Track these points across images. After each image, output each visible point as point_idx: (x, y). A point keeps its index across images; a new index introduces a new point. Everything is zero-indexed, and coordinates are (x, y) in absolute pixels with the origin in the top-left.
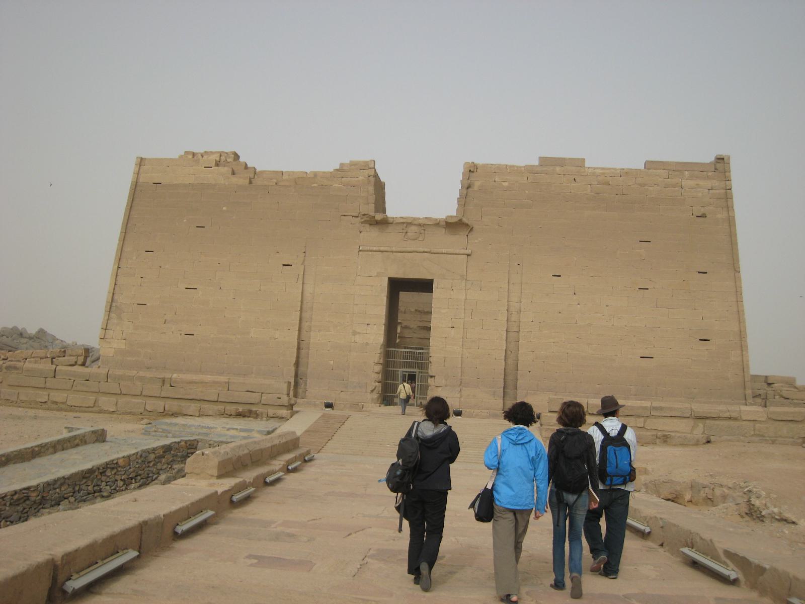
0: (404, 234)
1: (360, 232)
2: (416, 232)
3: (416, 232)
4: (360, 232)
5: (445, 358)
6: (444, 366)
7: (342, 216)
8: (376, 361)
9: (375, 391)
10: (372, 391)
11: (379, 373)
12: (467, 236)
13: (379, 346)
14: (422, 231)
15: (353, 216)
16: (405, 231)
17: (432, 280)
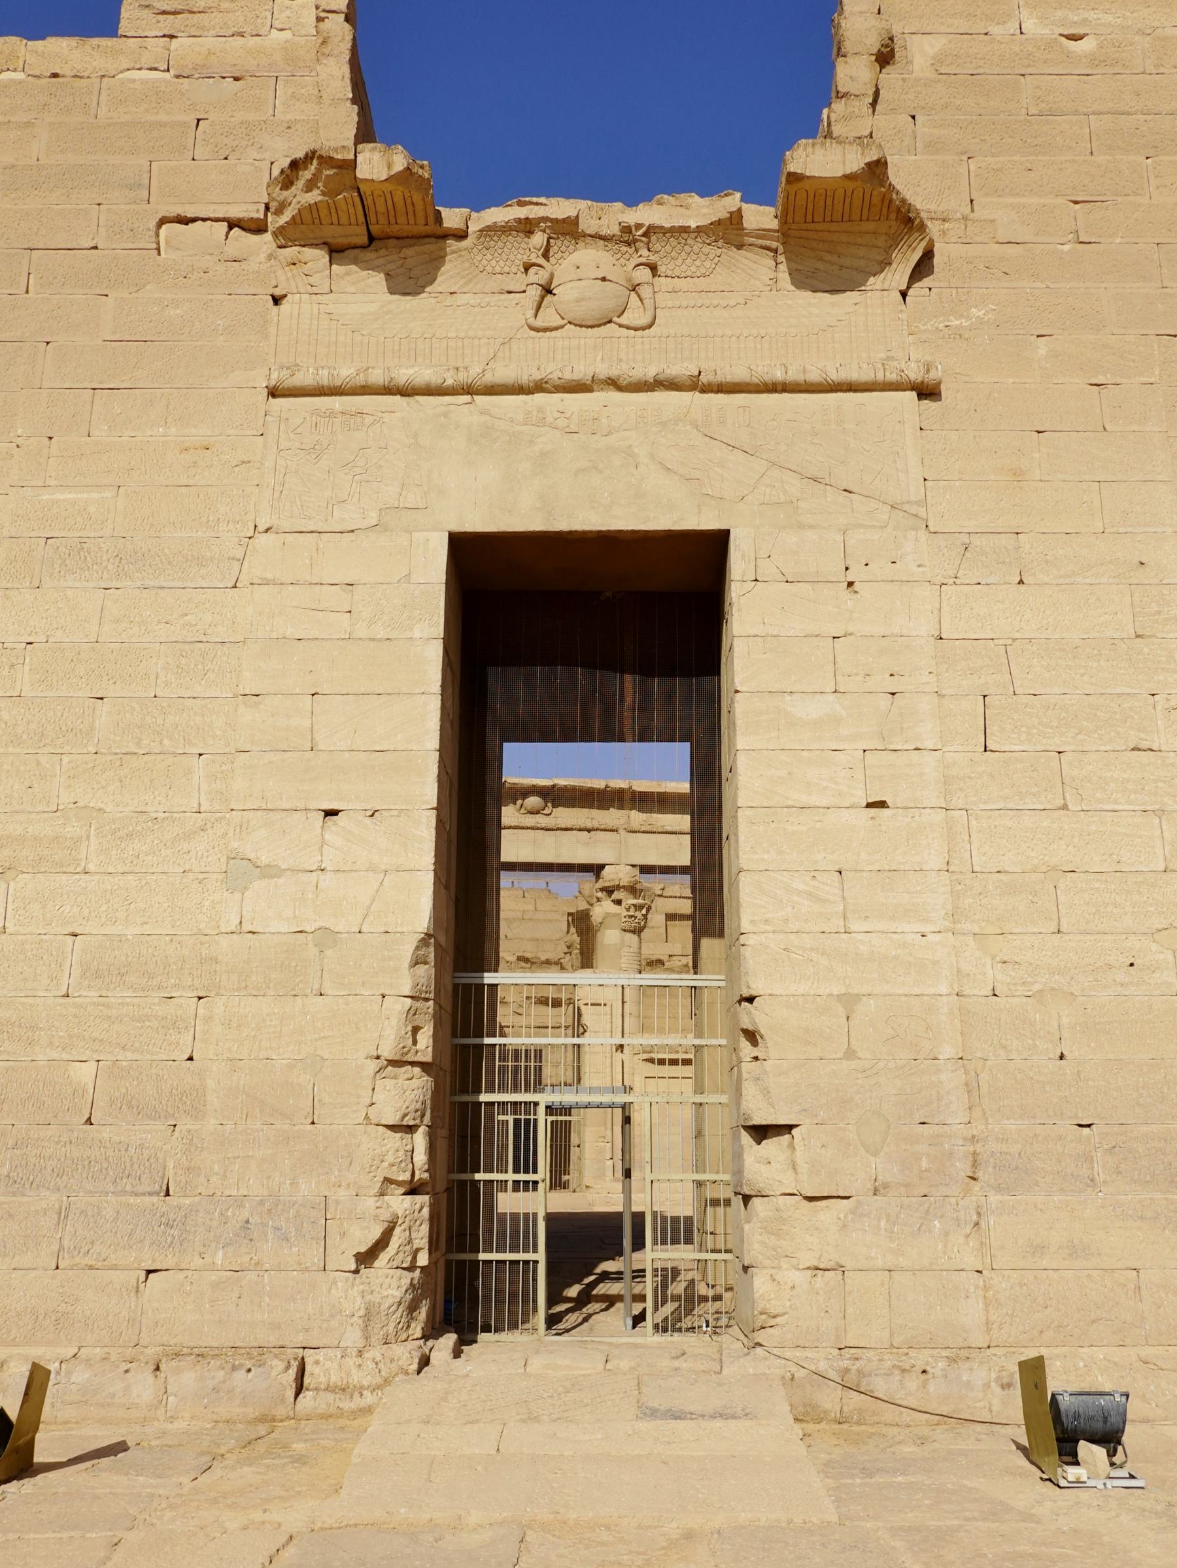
0: (535, 292)
1: (276, 300)
2: (604, 279)
3: (604, 279)
4: (276, 300)
5: (849, 1001)
6: (850, 1054)
7: (163, 221)
8: (388, 1052)
9: (383, 1258)
10: (366, 1258)
11: (411, 1129)
12: (904, 294)
13: (408, 950)
14: (644, 274)
15: (232, 224)
16: (537, 276)
17: (715, 545)
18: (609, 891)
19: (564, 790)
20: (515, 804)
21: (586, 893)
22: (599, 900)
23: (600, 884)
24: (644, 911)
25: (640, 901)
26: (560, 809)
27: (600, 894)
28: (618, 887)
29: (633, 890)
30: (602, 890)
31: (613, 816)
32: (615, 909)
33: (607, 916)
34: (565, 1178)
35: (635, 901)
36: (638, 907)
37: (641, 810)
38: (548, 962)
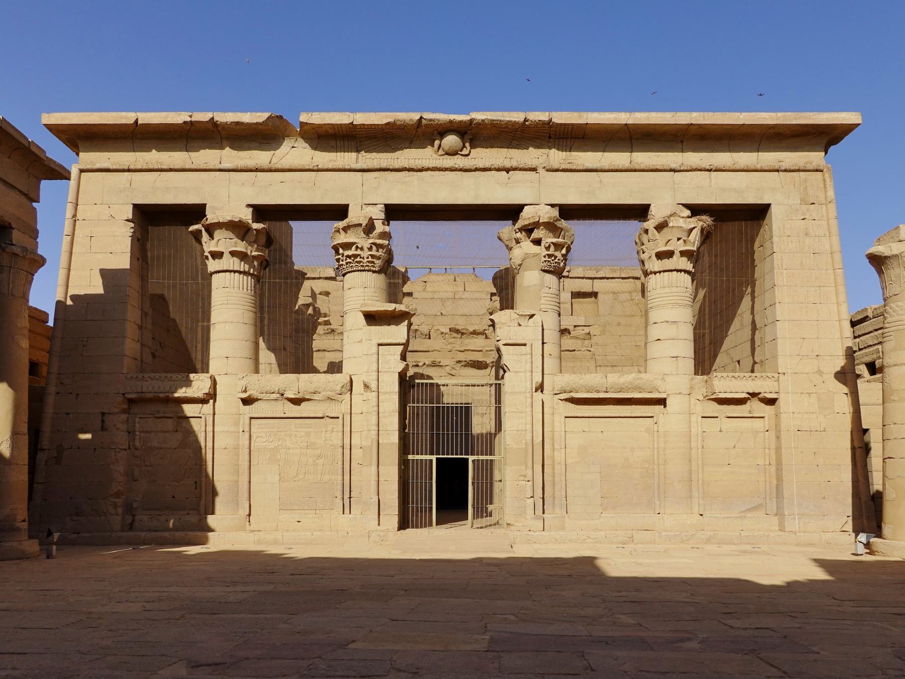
18: (528, 230)
19: (482, 124)
20: (433, 146)
21: (505, 236)
22: (518, 241)
23: (520, 224)
24: (564, 251)
25: (560, 240)
26: (479, 150)
27: (519, 235)
28: (536, 225)
29: (551, 227)
30: (520, 230)
31: (532, 155)
32: (536, 249)
33: (526, 256)
34: (490, 507)
35: (555, 240)
36: (558, 246)
37: (560, 148)
38: (475, 333)
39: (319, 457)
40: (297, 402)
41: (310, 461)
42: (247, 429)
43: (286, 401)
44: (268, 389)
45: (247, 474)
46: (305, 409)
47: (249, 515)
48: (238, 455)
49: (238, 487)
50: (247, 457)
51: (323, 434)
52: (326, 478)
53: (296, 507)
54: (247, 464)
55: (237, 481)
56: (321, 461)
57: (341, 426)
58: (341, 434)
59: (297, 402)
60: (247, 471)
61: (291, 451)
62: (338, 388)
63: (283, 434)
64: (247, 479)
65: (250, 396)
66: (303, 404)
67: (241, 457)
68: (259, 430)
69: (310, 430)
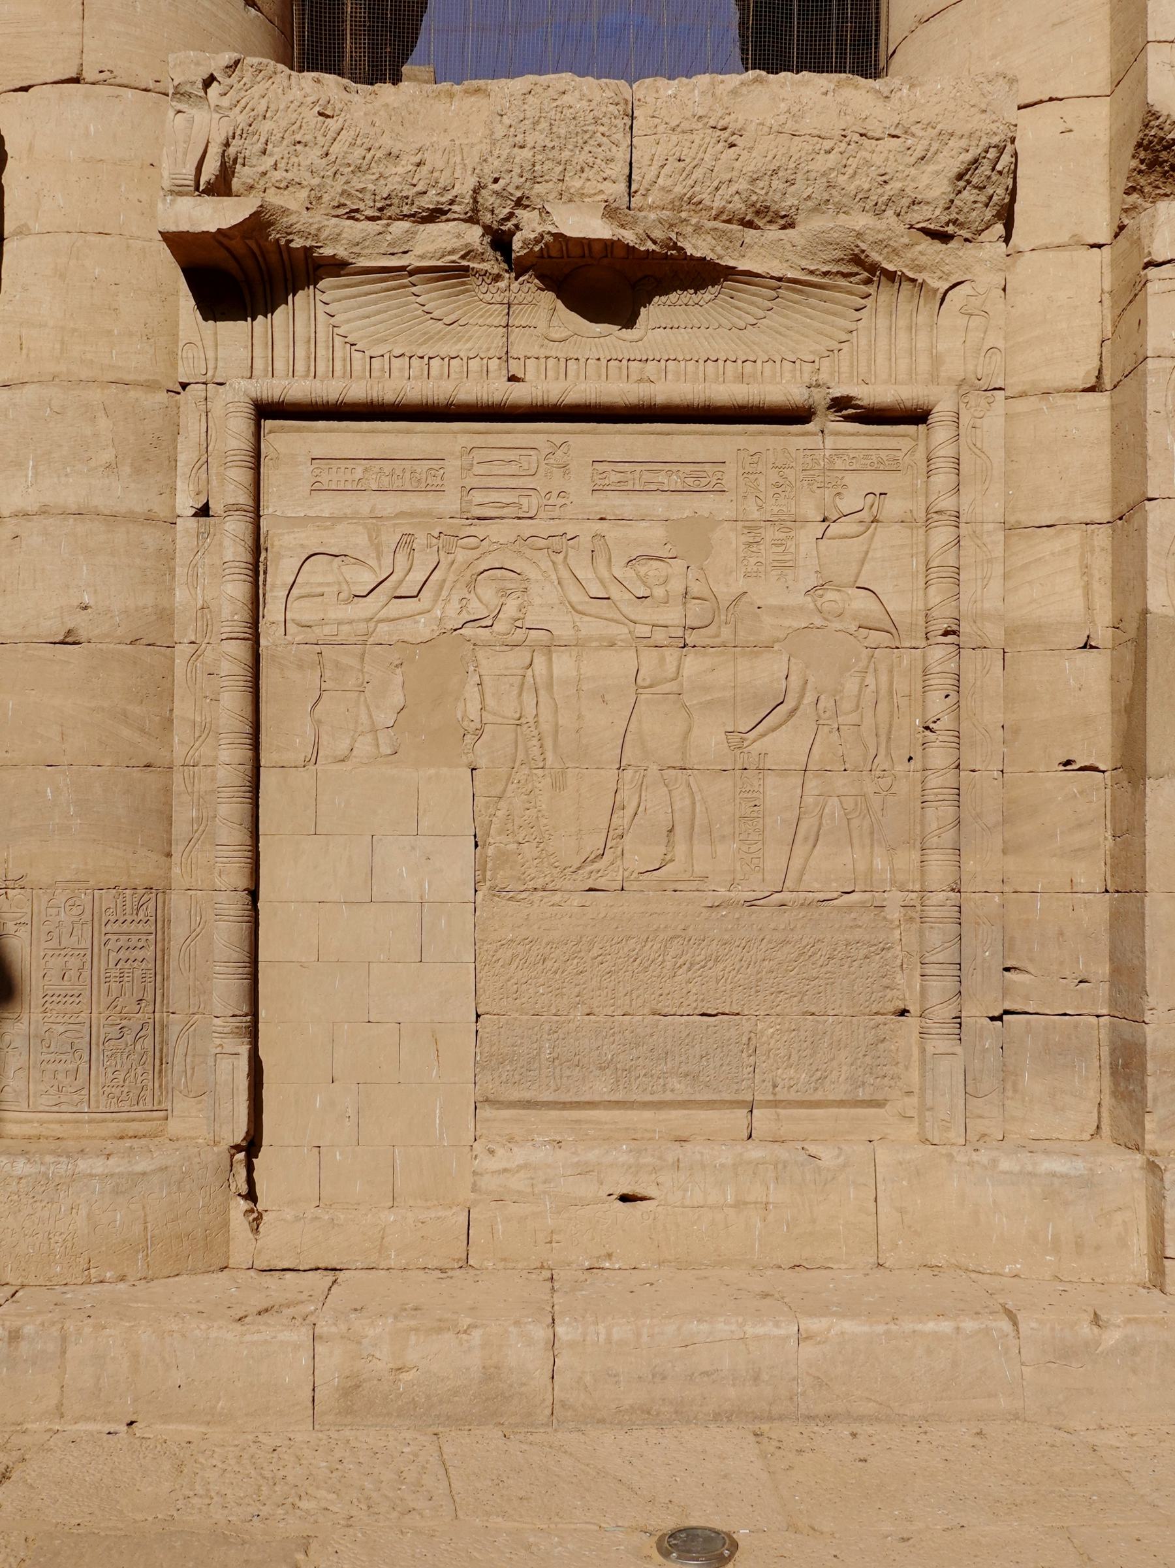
39: (776, 707)
40: (607, 282)
41: (710, 738)
42: (230, 489)
43: (527, 290)
44: (394, 179)
45: (232, 835)
46: (670, 349)
47: (252, 1146)
48: (162, 690)
49: (161, 923)
50: (231, 704)
51: (806, 537)
52: (828, 866)
53: (600, 1088)
54: (229, 756)
55: (158, 890)
56: (784, 744)
57: (942, 480)
58: (942, 535)
59: (607, 282)
60: (229, 811)
61: (563, 665)
62: (933, 183)
63: (498, 532)
64: (235, 876)
65: (258, 223)
66: (654, 313)
67: (183, 708)
68: (326, 506)
69: (706, 505)
